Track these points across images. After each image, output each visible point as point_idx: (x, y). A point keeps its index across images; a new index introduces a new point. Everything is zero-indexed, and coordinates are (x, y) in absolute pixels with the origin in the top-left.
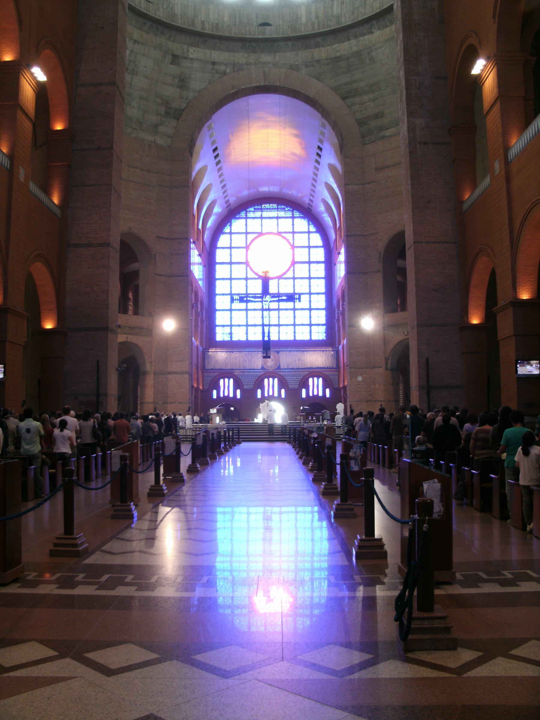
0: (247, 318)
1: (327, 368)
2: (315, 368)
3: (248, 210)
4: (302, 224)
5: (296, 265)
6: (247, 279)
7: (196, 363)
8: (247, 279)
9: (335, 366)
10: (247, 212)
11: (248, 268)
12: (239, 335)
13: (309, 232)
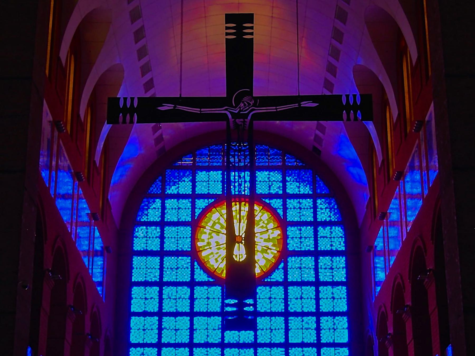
6: (192, 284)
8: (192, 284)
13: (314, 197)
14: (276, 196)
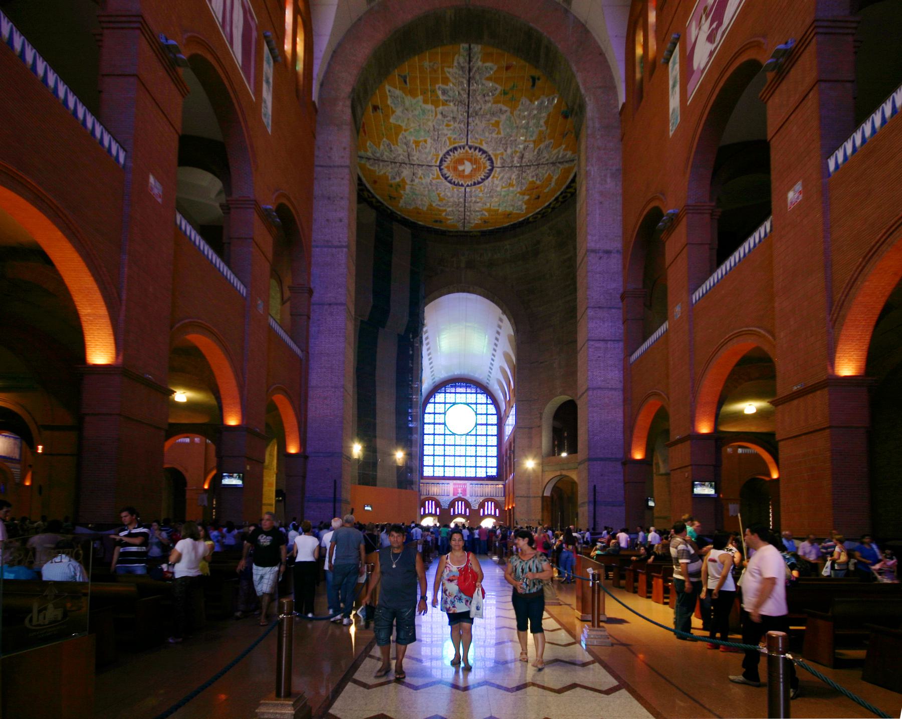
4: (482, 398)
5: (478, 426)
10: (445, 388)
12: (439, 472)
13: (487, 404)
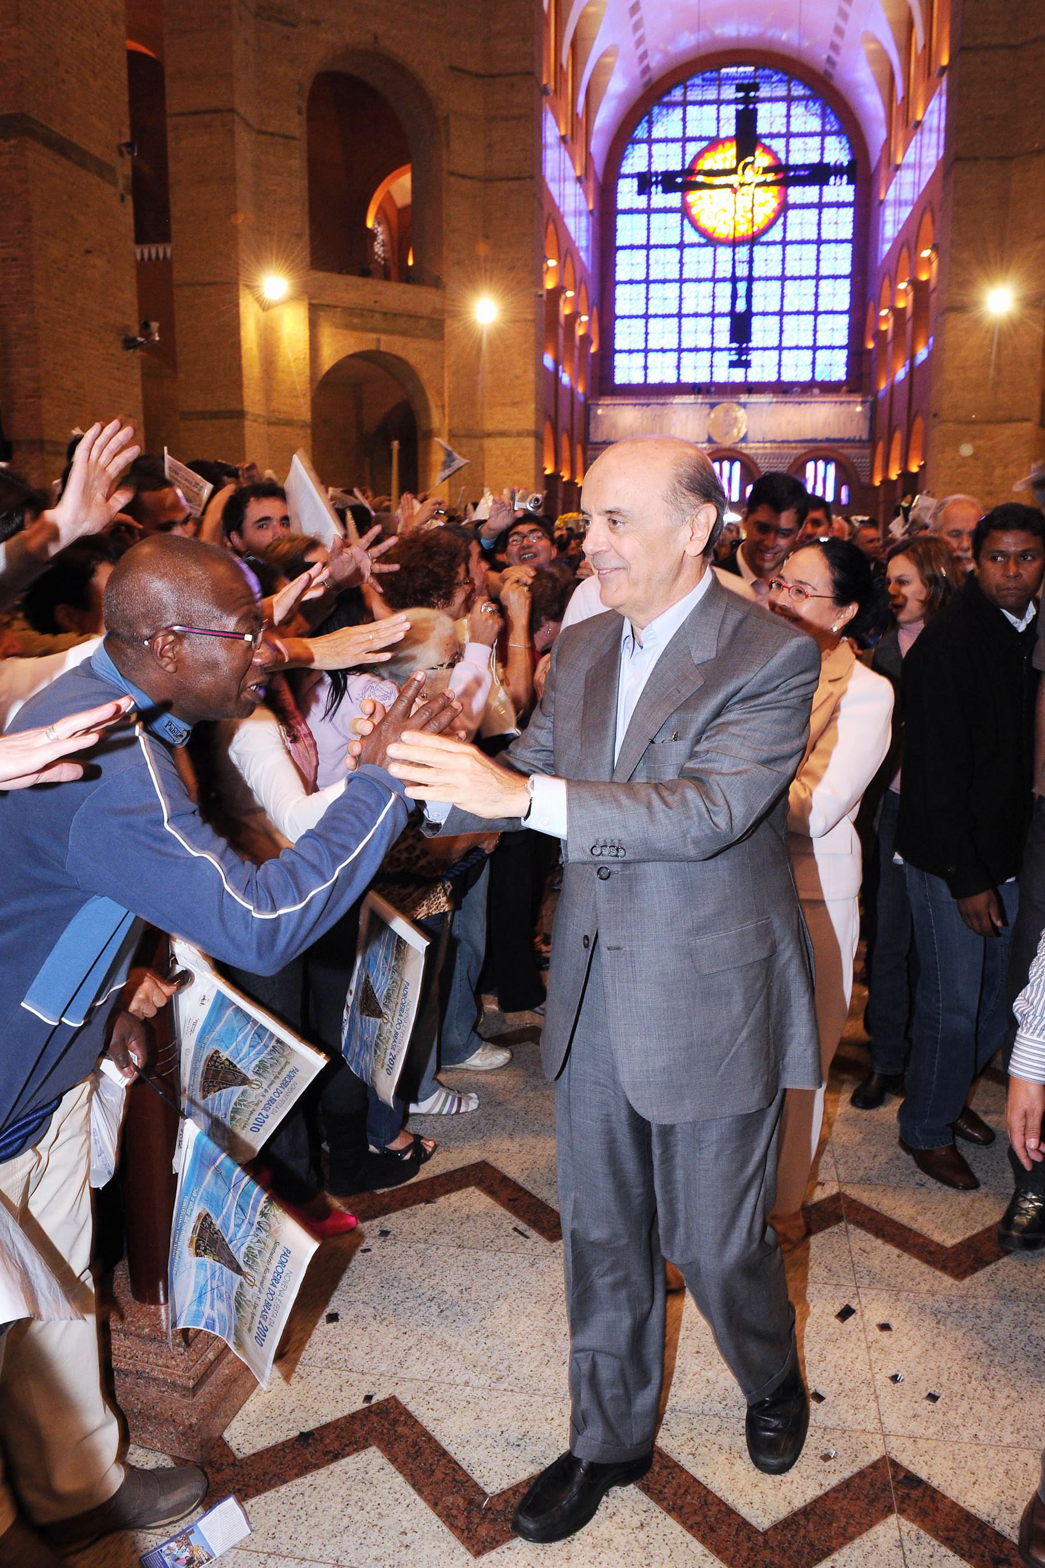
0: (680, 333)
1: (848, 441)
2: (821, 441)
3: (689, 83)
5: (791, 213)
6: (681, 246)
7: (568, 426)
8: (681, 246)
9: (865, 436)
10: (686, 88)
11: (686, 222)
12: (662, 371)
14: (779, 135)
